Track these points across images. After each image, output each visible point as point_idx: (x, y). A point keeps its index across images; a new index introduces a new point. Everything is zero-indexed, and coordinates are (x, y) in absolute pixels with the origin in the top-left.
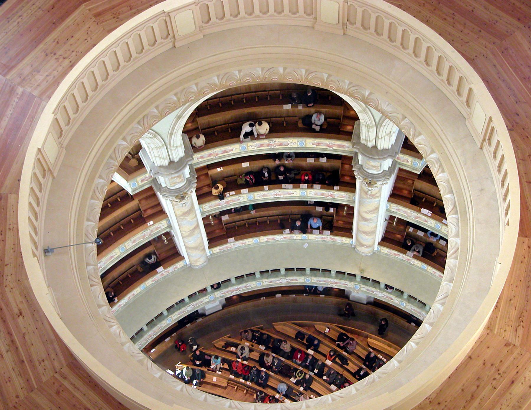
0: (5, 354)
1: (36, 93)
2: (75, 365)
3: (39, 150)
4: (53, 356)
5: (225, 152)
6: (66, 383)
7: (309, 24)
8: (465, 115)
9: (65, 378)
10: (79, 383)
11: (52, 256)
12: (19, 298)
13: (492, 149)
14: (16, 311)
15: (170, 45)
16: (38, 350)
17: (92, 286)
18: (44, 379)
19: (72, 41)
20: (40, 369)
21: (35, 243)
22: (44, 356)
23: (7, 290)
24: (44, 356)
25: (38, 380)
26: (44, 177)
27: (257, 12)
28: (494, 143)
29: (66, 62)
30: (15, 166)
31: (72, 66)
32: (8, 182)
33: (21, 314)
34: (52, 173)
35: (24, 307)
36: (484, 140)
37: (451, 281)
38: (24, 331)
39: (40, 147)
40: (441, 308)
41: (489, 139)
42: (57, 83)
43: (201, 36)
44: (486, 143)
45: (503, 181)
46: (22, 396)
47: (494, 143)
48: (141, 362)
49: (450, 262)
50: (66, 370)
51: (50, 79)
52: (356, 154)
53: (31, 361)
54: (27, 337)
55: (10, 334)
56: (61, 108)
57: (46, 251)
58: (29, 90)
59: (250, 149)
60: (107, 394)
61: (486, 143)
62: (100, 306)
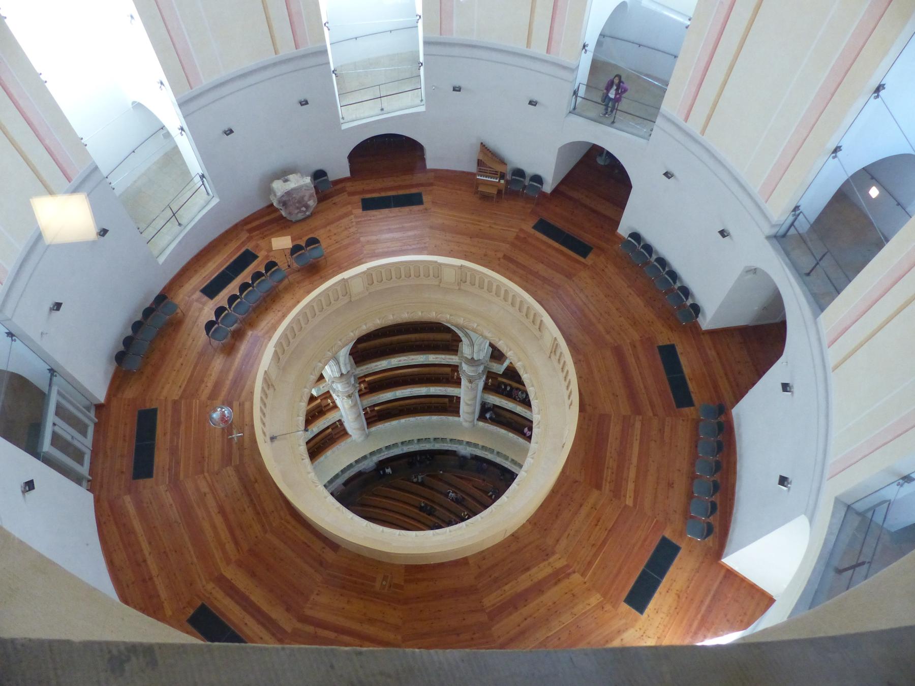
0: (247, 509)
1: (260, 334)
6: (289, 527)
7: (437, 283)
9: (288, 523)
11: (276, 442)
13: (557, 357)
14: (253, 479)
15: (348, 300)
18: (274, 525)
21: (264, 433)
27: (403, 276)
28: (558, 354)
29: (280, 314)
30: (249, 383)
31: (284, 316)
32: (244, 394)
33: (256, 481)
40: (532, 461)
42: (274, 328)
44: (553, 355)
45: (565, 378)
47: (558, 354)
48: (338, 508)
50: (289, 518)
51: (269, 325)
56: (279, 344)
61: (553, 355)
62: (309, 473)
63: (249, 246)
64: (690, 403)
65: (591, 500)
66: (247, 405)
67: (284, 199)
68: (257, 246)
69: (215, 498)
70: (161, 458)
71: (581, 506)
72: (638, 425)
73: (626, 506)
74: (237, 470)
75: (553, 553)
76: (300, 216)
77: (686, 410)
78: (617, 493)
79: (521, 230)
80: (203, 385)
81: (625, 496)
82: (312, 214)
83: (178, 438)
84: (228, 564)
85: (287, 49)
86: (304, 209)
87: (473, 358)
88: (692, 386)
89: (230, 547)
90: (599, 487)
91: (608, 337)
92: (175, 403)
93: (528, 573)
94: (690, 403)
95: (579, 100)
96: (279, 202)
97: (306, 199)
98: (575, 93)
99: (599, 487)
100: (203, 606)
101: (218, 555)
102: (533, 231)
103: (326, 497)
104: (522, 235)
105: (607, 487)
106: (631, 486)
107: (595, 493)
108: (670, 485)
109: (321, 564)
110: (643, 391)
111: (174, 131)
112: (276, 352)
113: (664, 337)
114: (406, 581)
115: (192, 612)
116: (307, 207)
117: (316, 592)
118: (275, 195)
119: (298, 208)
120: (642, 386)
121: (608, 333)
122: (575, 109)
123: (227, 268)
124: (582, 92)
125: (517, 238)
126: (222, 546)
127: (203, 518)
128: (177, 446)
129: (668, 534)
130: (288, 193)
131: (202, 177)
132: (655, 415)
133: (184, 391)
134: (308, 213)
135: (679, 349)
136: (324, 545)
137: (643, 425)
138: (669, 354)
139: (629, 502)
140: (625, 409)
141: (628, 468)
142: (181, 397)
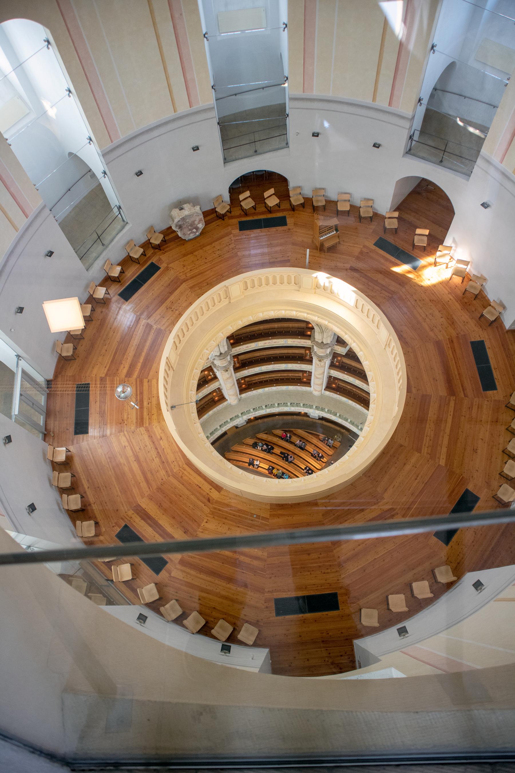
0: (155, 459)
1: (163, 328)
2: (189, 464)
3: (167, 358)
4: (178, 459)
5: (247, 347)
6: (185, 472)
8: (377, 333)
9: (185, 470)
10: (192, 472)
11: (175, 410)
12: (160, 431)
13: (391, 350)
14: (159, 437)
16: (171, 457)
17: (195, 423)
18: (175, 471)
19: (179, 301)
20: (173, 466)
21: (166, 403)
22: (174, 460)
23: (154, 427)
24: (174, 460)
25: (172, 470)
26: (169, 369)
30: (155, 365)
32: (151, 373)
33: (161, 439)
34: (173, 368)
35: (163, 435)
36: (386, 345)
37: (372, 415)
38: (163, 447)
39: (168, 356)
40: (368, 429)
41: (389, 344)
43: (243, 296)
46: (164, 480)
48: (221, 460)
49: (371, 406)
50: (185, 466)
52: (313, 346)
53: (168, 462)
54: (165, 450)
55: (156, 449)
57: (173, 407)
58: (159, 327)
59: (260, 345)
60: (206, 477)
62: (199, 433)
63: (154, 260)
64: (494, 388)
65: (413, 460)
66: (154, 382)
67: (180, 223)
68: (160, 260)
69: (132, 450)
70: (93, 419)
71: (405, 464)
72: (452, 404)
73: (439, 465)
74: (147, 430)
75: (383, 498)
76: (192, 236)
77: (490, 393)
78: (433, 455)
79: (365, 246)
80: (122, 366)
81: (439, 458)
82: (201, 234)
83: (105, 406)
84: (143, 497)
85: (183, 108)
86: (194, 230)
87: (322, 342)
88: (496, 374)
89: (144, 485)
90: (419, 450)
91: (431, 334)
92: (102, 379)
93: (363, 513)
94: (494, 388)
95: (414, 143)
96: (176, 226)
97: (196, 222)
98: (411, 137)
99: (419, 450)
100: (126, 526)
101: (135, 491)
102: (374, 247)
103: (212, 452)
104: (365, 250)
105: (425, 450)
106: (444, 450)
107: (417, 455)
108: (475, 451)
109: (209, 500)
110: (458, 377)
111: (99, 175)
112: (174, 342)
113: (477, 334)
114: (270, 515)
115: (119, 530)
116: (197, 228)
117: (205, 521)
118: (173, 221)
119: (190, 230)
120: (456, 373)
121: (432, 330)
122: (410, 150)
123: (138, 277)
124: (416, 137)
125: (361, 253)
126: (138, 484)
127: (124, 465)
128: (104, 411)
129: (470, 487)
130: (183, 219)
131: (119, 208)
132: (466, 396)
133: (108, 370)
134: (197, 234)
135: (487, 344)
136: (211, 487)
137: (455, 404)
138: (479, 349)
139: (442, 462)
140: (443, 391)
141: (443, 437)
142: (106, 375)
